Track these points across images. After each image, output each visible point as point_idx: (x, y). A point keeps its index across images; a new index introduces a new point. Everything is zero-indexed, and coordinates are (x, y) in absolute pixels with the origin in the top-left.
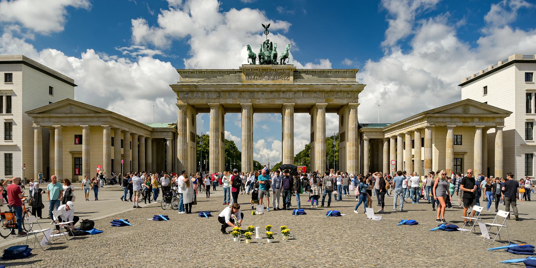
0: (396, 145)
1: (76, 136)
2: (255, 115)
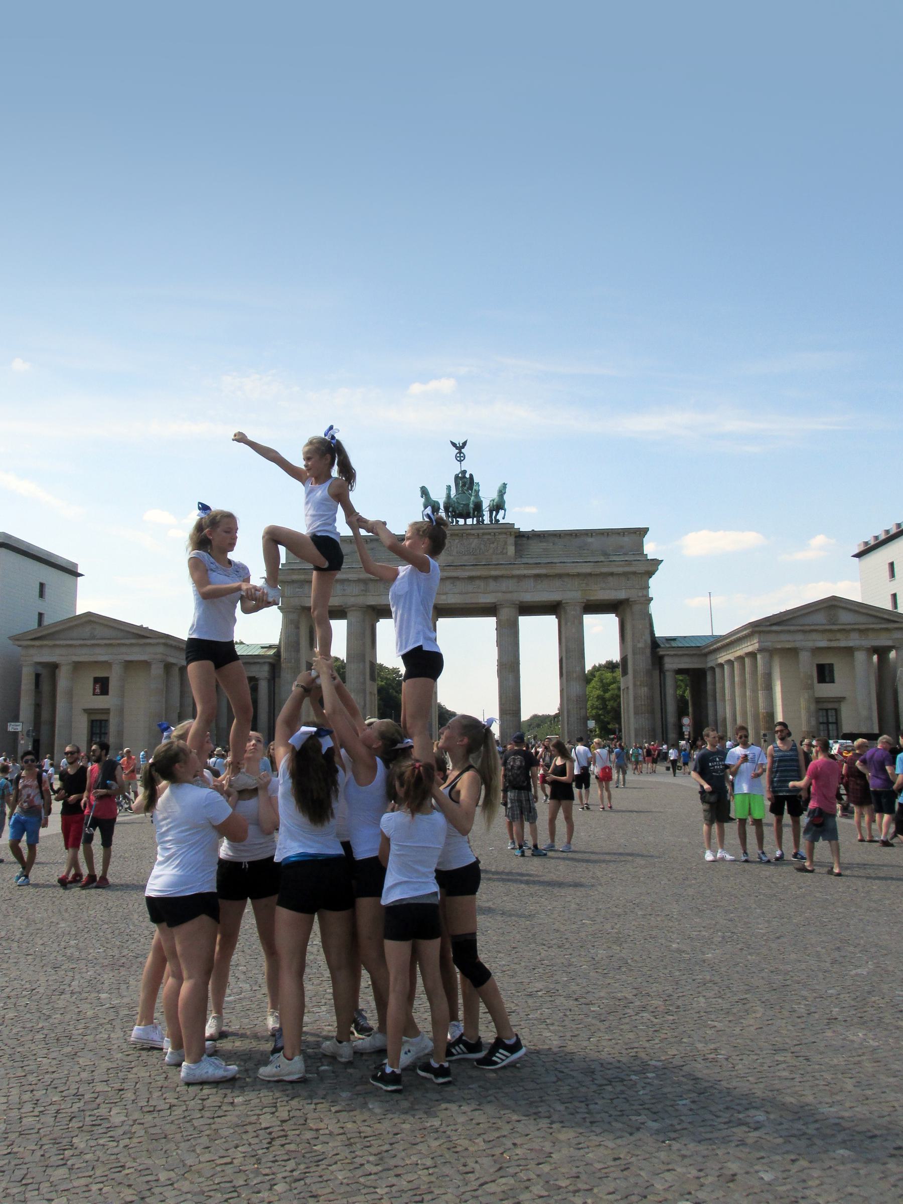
0: (714, 684)
1: (97, 680)
2: (442, 622)
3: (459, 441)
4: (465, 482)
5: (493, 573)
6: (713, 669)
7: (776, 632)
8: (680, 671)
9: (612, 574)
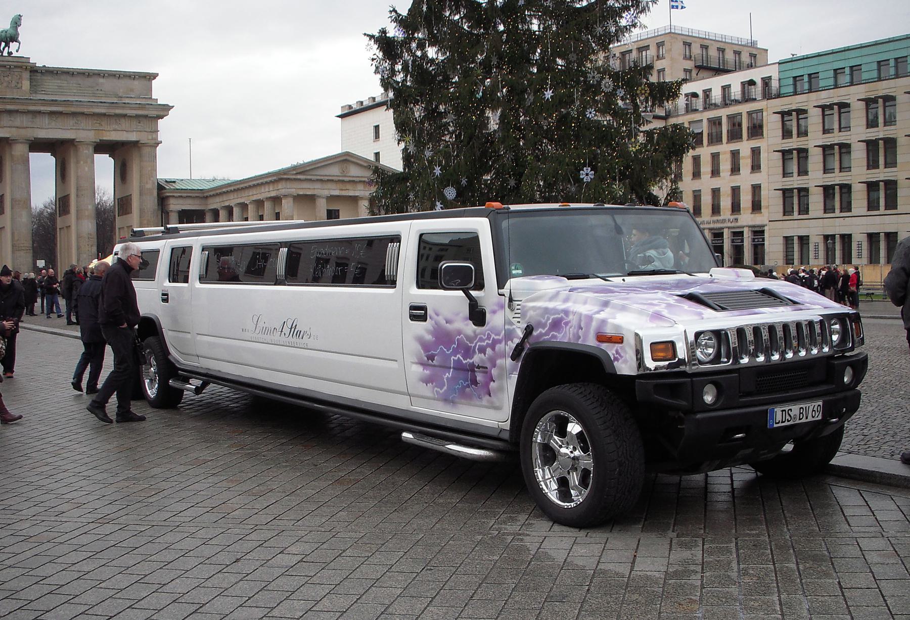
5: (9, 107)
7: (300, 180)
9: (125, 116)
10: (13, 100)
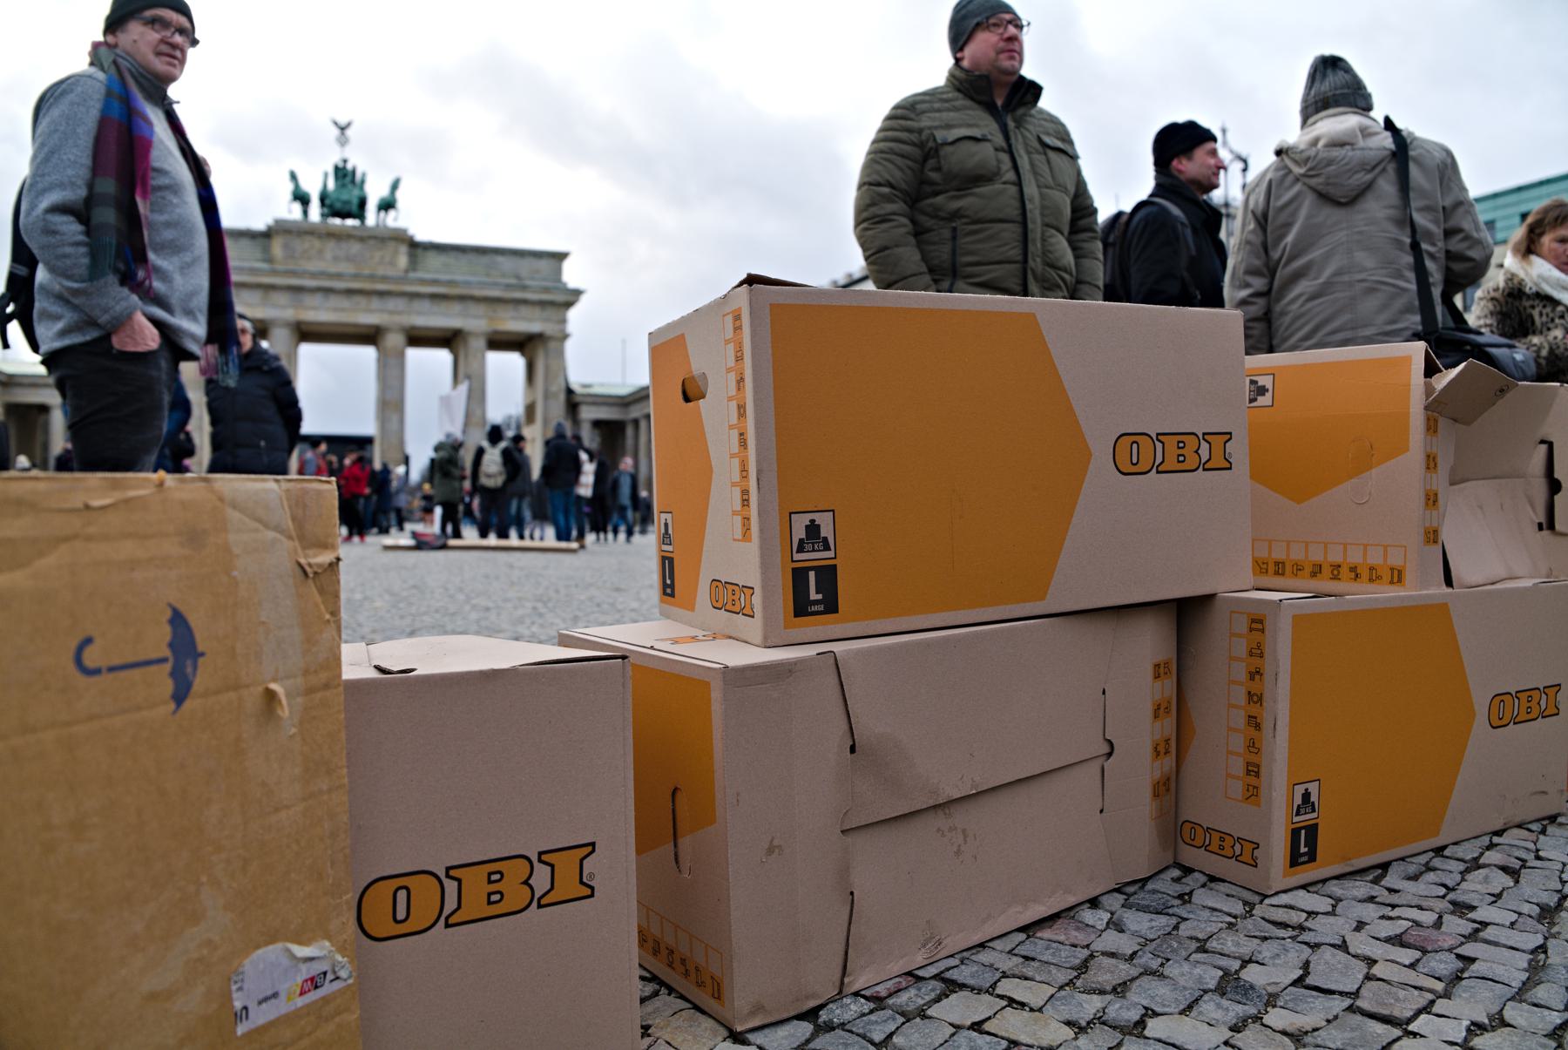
3: (343, 122)
4: (343, 174)
6: (636, 422)
8: (597, 424)
9: (525, 302)
10: (385, 279)
